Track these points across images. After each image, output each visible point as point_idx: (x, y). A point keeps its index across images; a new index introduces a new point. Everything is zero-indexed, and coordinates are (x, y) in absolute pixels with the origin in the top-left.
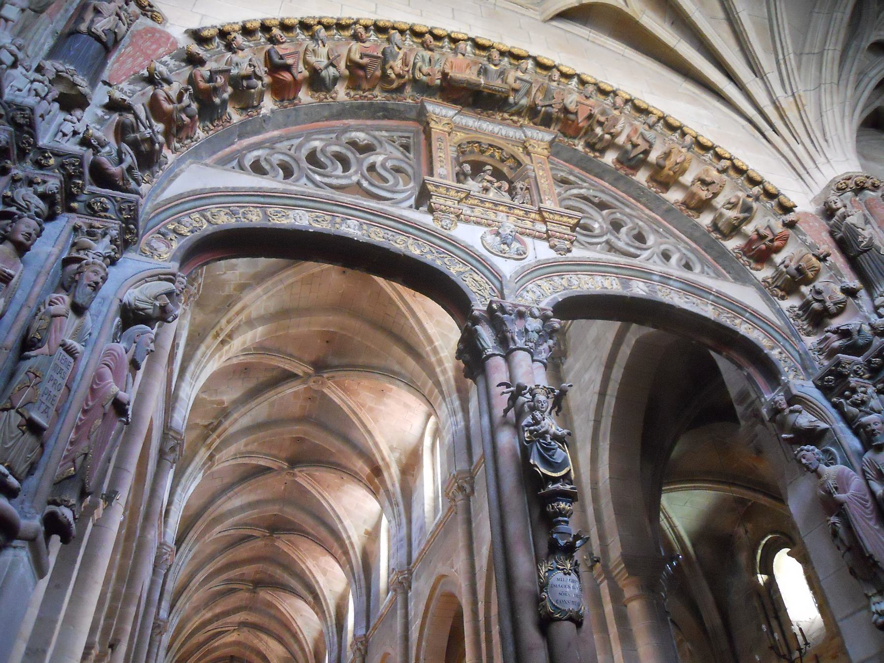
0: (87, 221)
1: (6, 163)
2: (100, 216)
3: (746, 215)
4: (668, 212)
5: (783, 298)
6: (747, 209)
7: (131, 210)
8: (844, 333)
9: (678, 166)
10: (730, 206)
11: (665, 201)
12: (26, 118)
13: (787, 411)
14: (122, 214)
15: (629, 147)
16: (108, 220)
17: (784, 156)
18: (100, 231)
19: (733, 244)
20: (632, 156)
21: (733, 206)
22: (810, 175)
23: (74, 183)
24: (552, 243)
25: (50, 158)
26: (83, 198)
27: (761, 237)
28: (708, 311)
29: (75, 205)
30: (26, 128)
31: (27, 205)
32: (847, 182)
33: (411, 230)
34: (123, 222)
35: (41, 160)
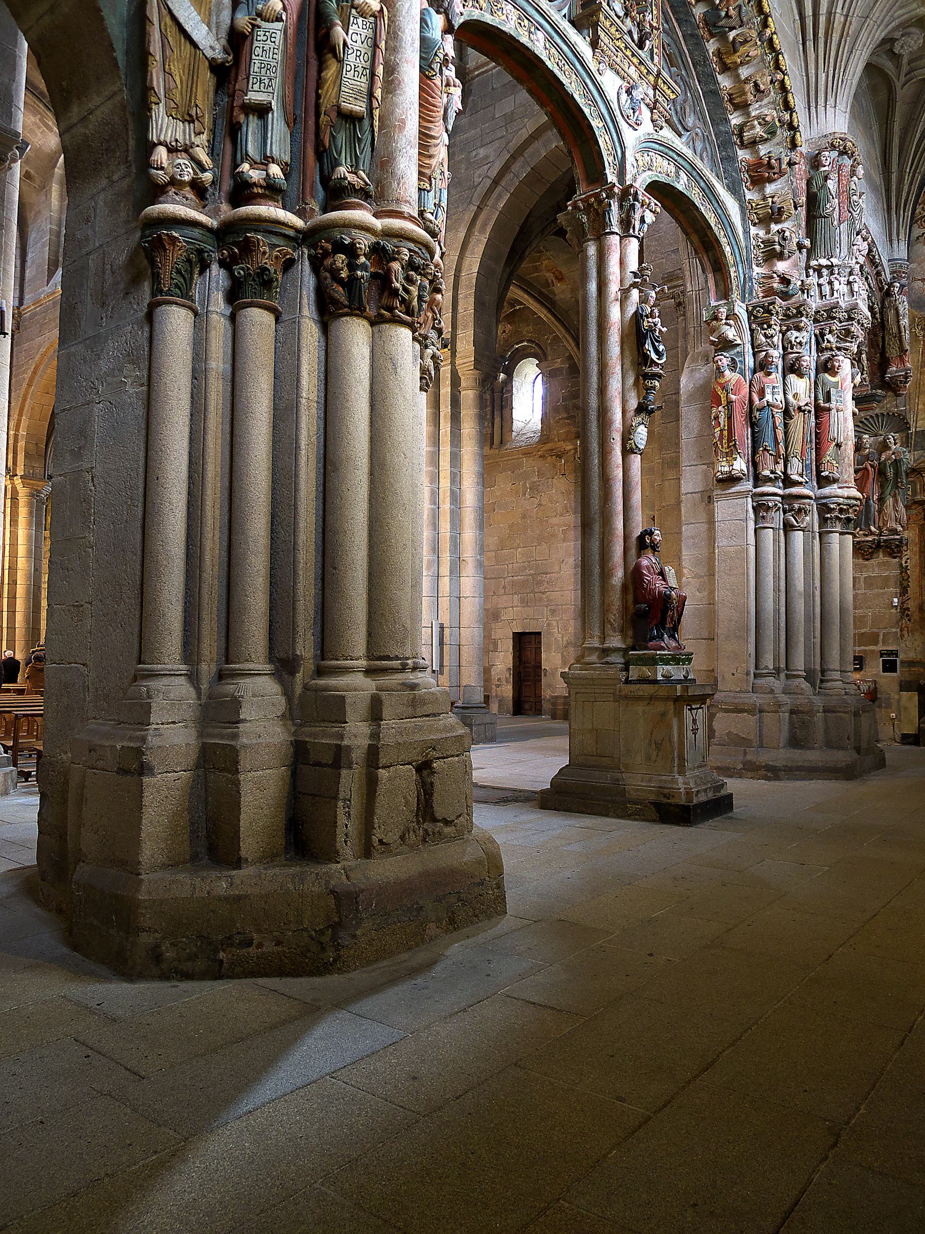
3: (769, 136)
4: (713, 93)
5: (755, 224)
6: (773, 133)
8: (785, 281)
9: (748, 59)
10: (763, 122)
11: (716, 82)
13: (724, 321)
15: (723, 14)
17: (807, 76)
19: (743, 155)
20: (720, 24)
21: (764, 123)
22: (817, 111)
24: (655, 117)
27: (770, 166)
28: (712, 220)
32: (841, 142)
33: (577, 64)
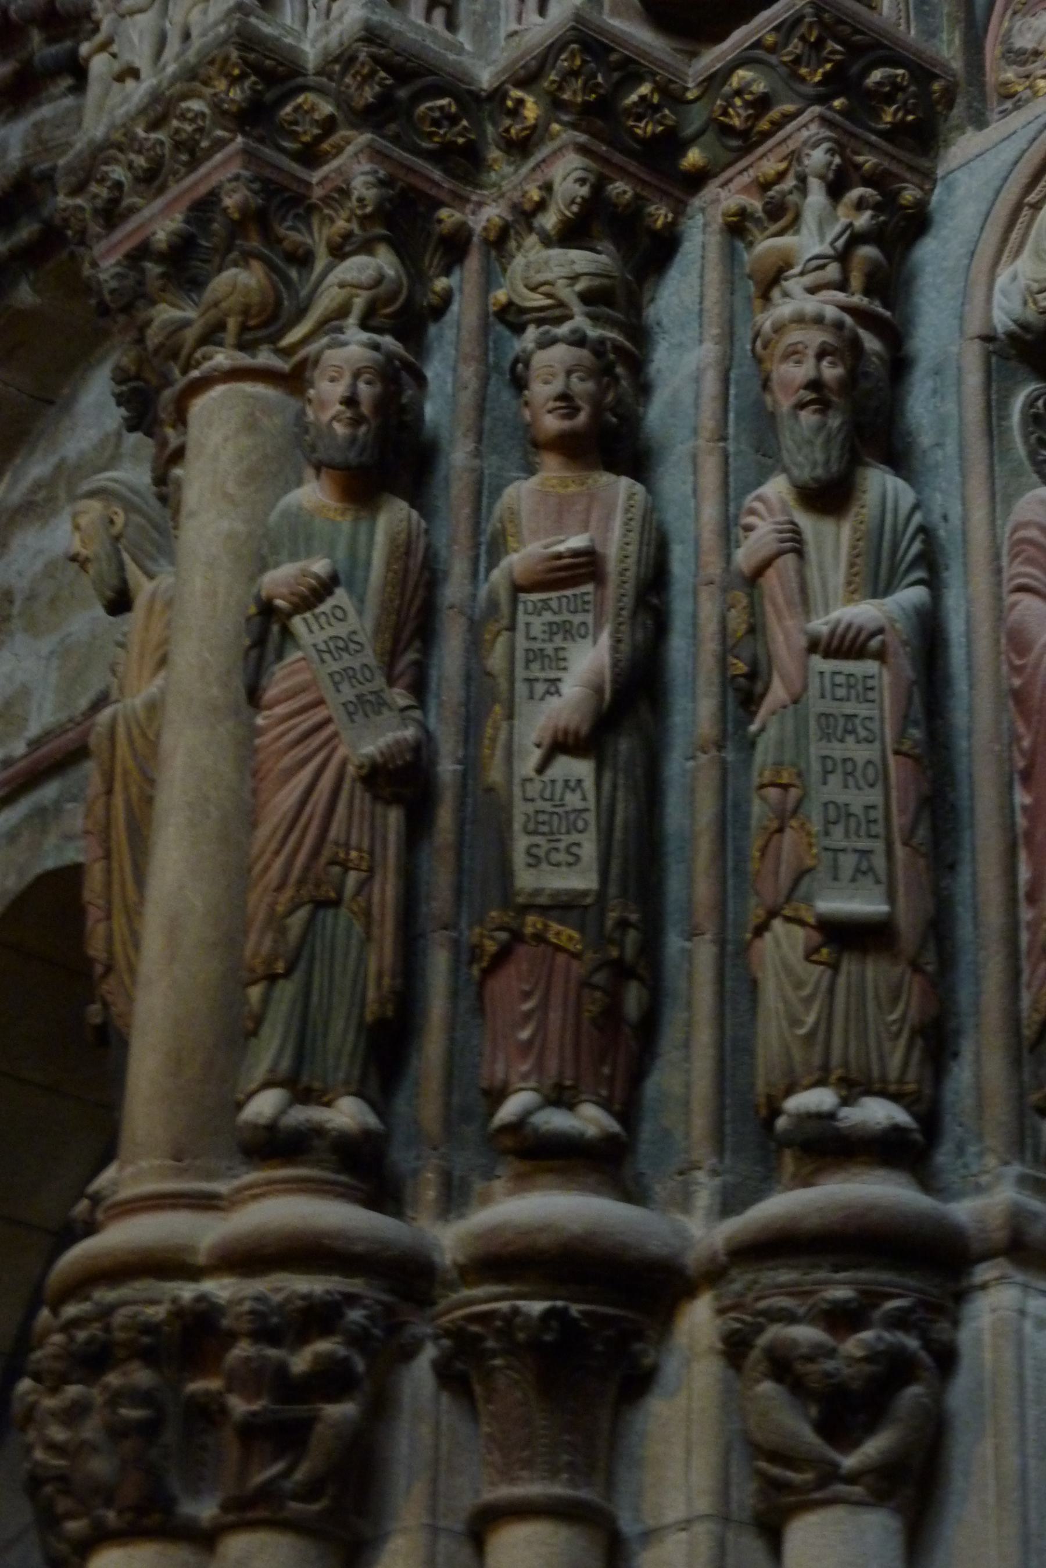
0: (745, 179)
1: (440, 221)
2: (766, 135)
7: (818, 45)
12: (373, 73)
14: (802, 80)
16: (789, 128)
18: (790, 182)
23: (628, 112)
25: (520, 102)
26: (696, 118)
29: (694, 157)
30: (402, 93)
31: (548, 295)
34: (823, 99)
35: (507, 130)
